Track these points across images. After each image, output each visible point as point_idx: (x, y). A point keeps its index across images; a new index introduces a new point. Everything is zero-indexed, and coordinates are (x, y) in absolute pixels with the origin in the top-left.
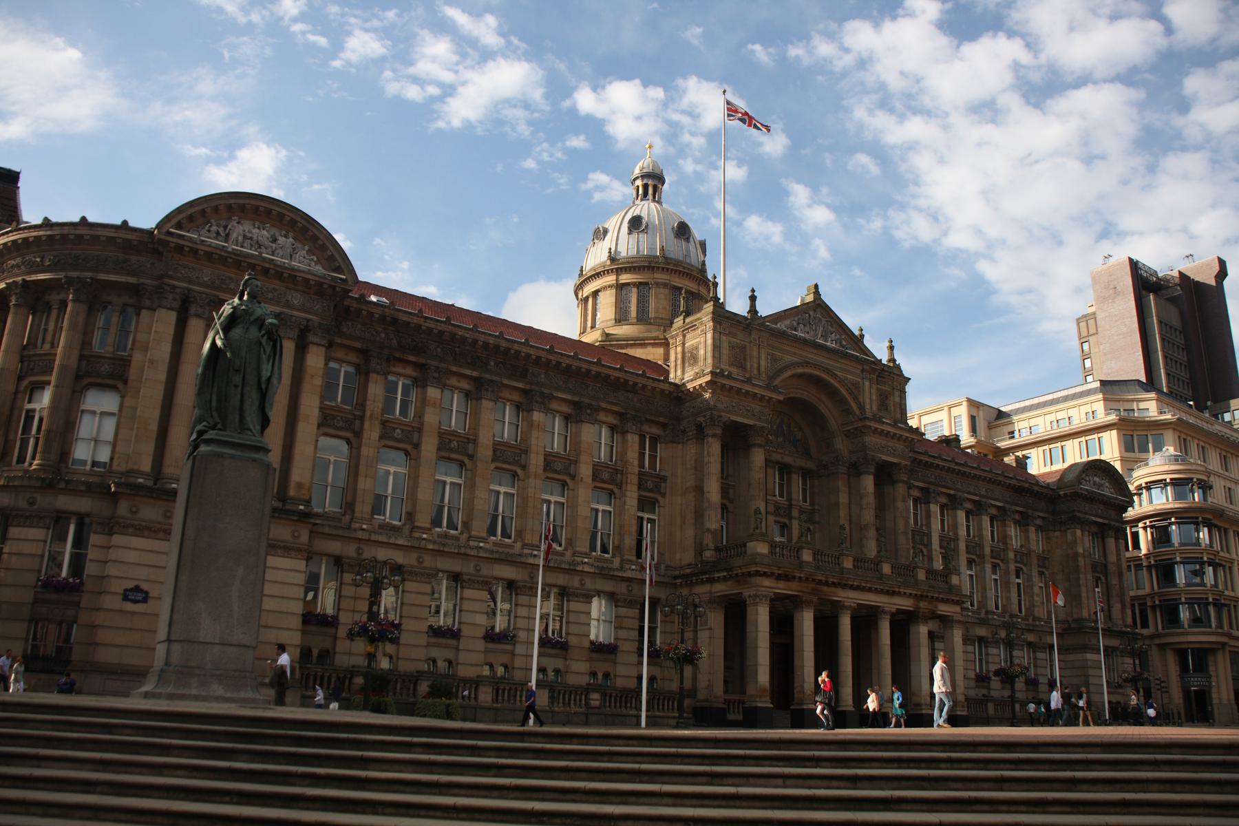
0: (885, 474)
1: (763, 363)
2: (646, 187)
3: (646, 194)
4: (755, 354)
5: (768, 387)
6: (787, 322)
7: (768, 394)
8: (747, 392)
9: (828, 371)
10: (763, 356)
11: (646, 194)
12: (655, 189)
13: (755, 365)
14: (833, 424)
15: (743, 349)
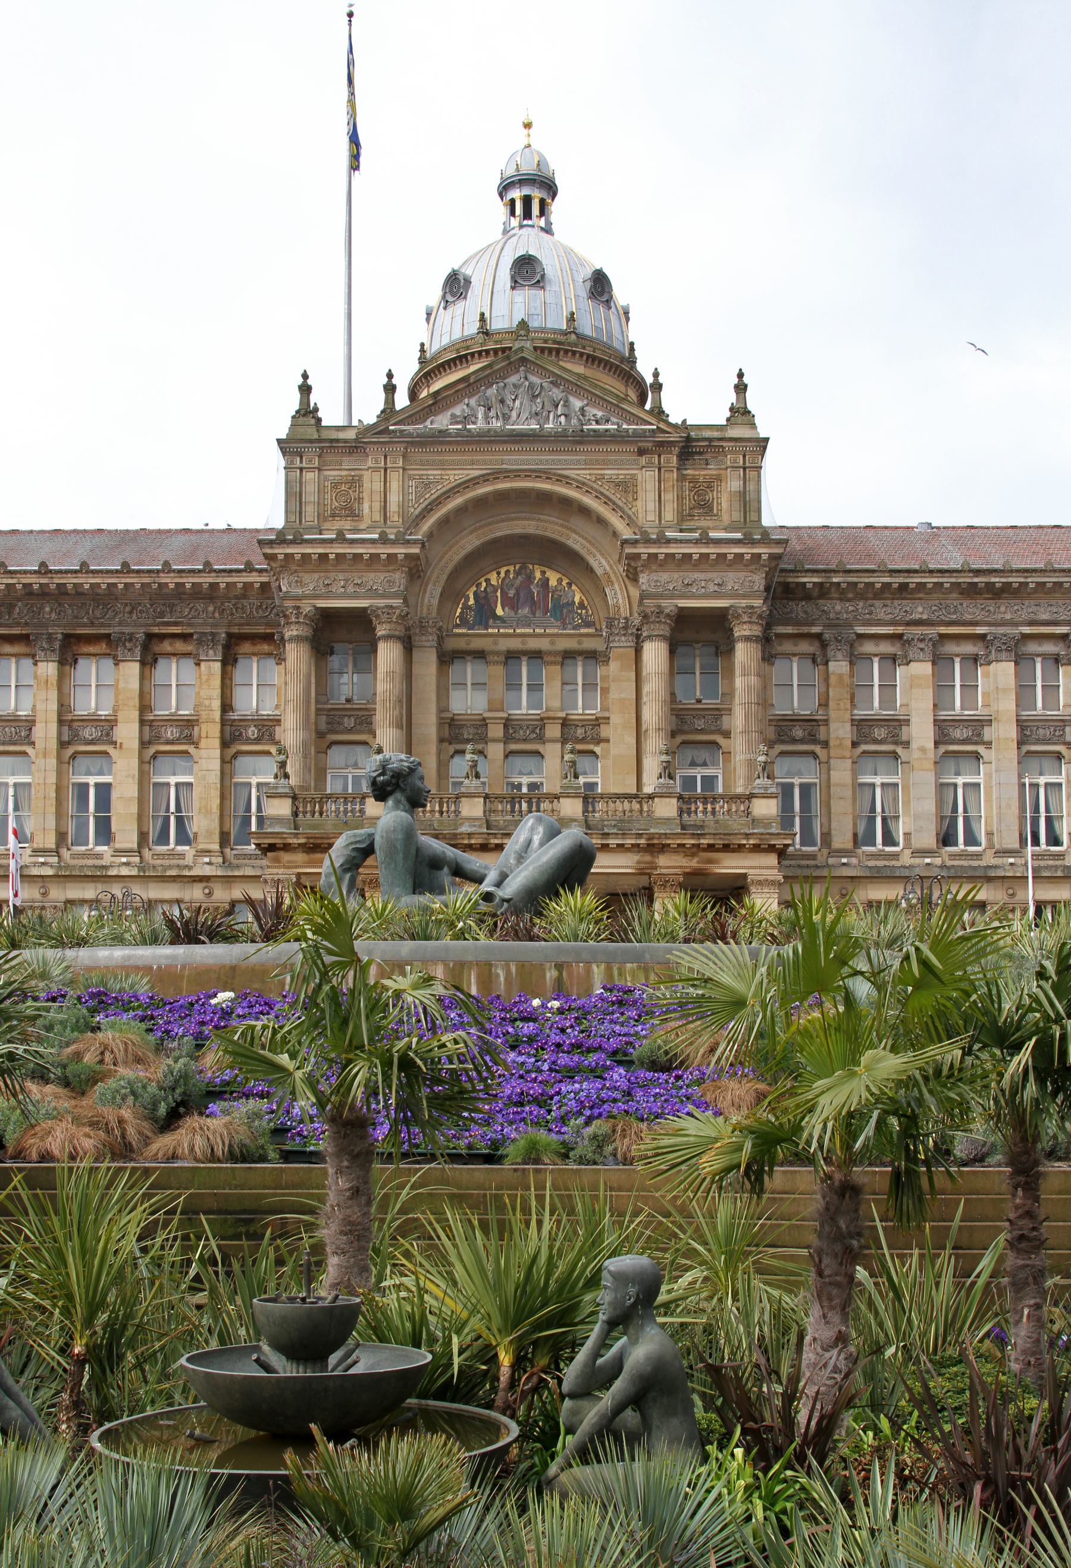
0: (699, 635)
1: (394, 499)
2: (527, 201)
3: (527, 214)
4: (378, 486)
5: (384, 540)
6: (457, 410)
7: (400, 550)
8: (338, 556)
9: (529, 474)
10: (395, 485)
11: (527, 214)
12: (543, 204)
13: (377, 506)
14: (600, 564)
15: (355, 482)
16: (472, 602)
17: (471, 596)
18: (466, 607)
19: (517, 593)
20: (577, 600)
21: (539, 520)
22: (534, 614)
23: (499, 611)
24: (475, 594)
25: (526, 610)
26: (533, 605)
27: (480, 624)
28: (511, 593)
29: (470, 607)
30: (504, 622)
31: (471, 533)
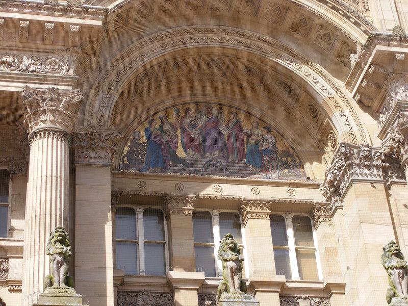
16: (143, 140)
17: (143, 133)
18: (136, 145)
19: (203, 134)
20: (280, 147)
21: (242, 35)
22: (227, 159)
23: (180, 153)
24: (148, 133)
25: (216, 154)
26: (225, 150)
27: (156, 164)
28: (195, 134)
29: (140, 146)
30: (188, 165)
31: (155, 40)
